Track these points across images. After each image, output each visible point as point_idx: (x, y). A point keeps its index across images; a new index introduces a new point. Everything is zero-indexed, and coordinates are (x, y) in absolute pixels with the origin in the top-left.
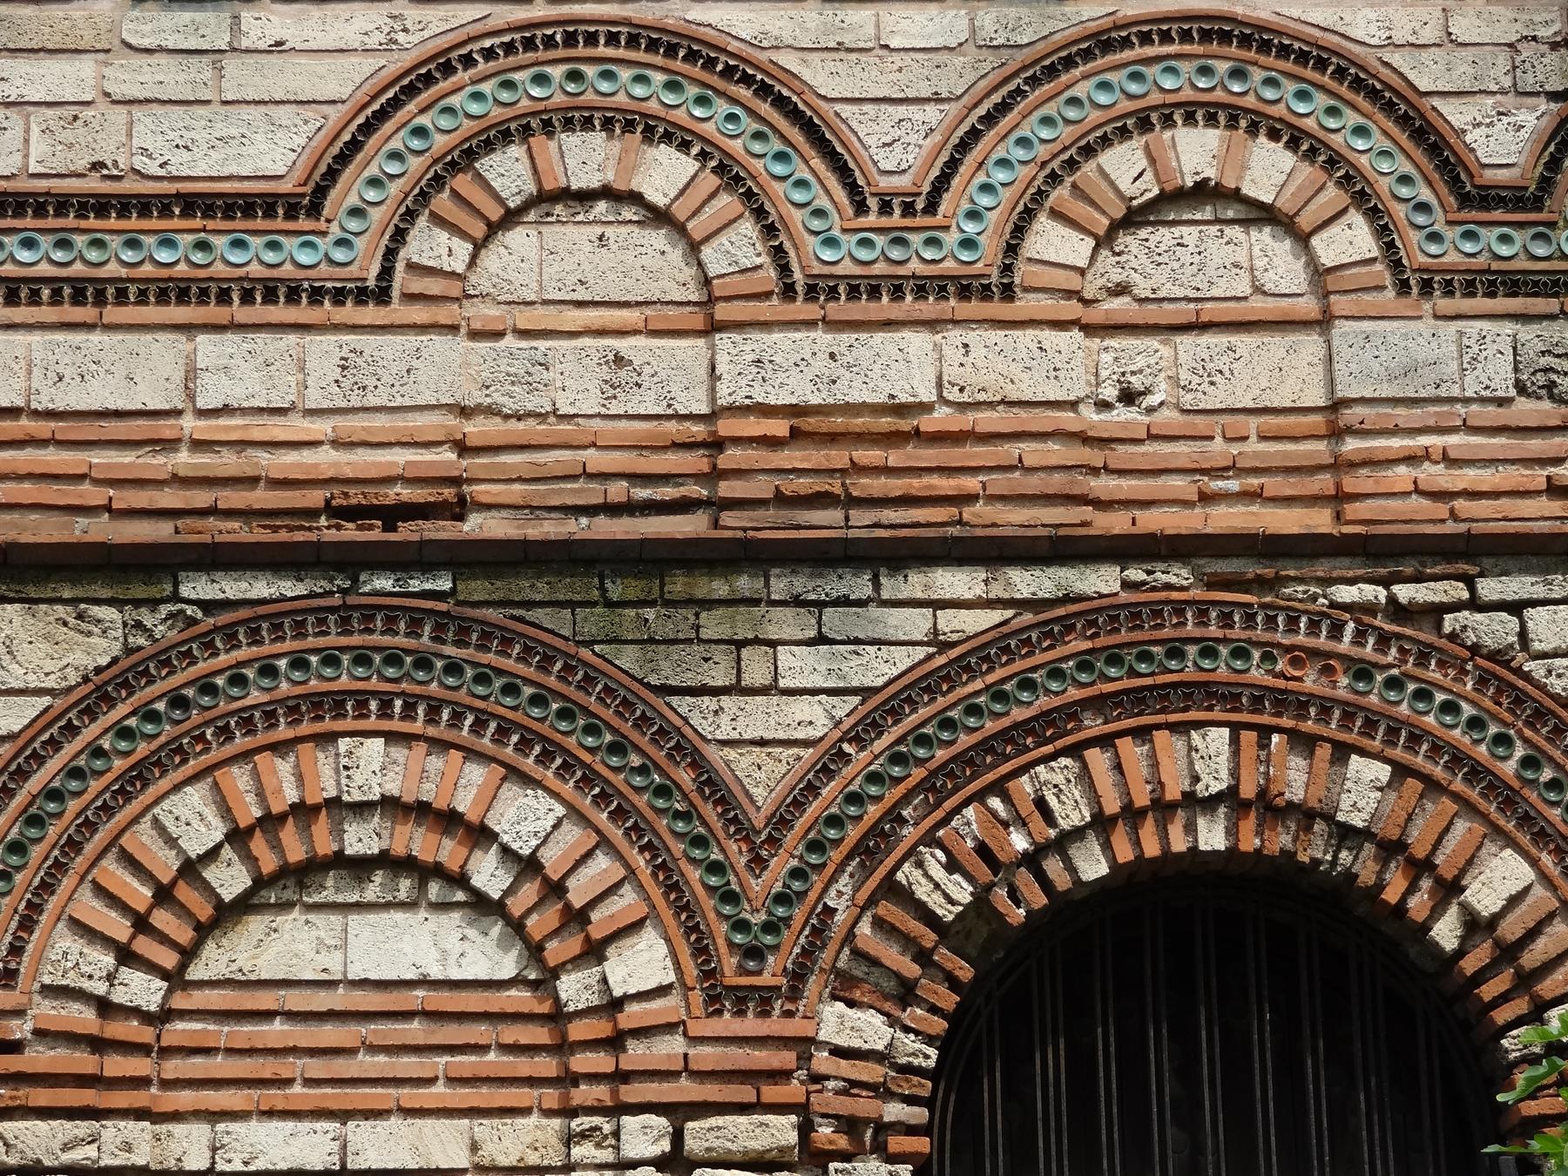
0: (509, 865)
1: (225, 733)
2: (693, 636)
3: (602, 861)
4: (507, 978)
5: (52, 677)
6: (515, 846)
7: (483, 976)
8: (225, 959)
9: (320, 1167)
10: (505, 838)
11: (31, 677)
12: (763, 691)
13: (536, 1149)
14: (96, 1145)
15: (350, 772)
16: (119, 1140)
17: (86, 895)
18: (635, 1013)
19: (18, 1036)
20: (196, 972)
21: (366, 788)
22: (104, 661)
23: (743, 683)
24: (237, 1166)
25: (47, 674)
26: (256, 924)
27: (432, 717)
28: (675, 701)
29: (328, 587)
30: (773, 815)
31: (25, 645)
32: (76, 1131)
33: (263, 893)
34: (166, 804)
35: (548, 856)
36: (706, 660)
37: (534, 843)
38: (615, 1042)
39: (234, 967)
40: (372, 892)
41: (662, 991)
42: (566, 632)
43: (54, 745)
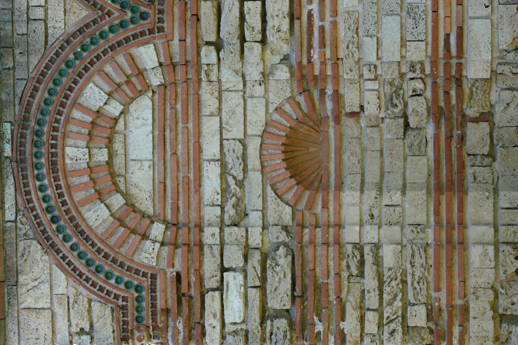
0: (111, 102)
1: (64, 203)
2: (25, 36)
3: (108, 69)
4: (151, 103)
5: (45, 264)
6: (104, 101)
7: (151, 111)
8: (146, 202)
9: (219, 168)
10: (102, 104)
11: (46, 272)
12: (46, 11)
13: (213, 93)
14: (213, 246)
15: (78, 159)
16: (211, 238)
17: (123, 250)
18: (165, 58)
19: (175, 273)
20: (151, 211)
21: (84, 154)
22: (39, 247)
23: (43, 18)
24: (219, 197)
25: (44, 266)
26: (133, 191)
27: (55, 129)
28: (50, 43)
29: (10, 167)
30: (91, 8)
31: (34, 274)
32: (208, 253)
33: (122, 188)
34: (91, 224)
35: (108, 89)
36: (35, 31)
37: (103, 94)
38: (174, 66)
39: (149, 199)
40: (121, 151)
41: (156, 49)
42: (25, 82)
43: (69, 264)
